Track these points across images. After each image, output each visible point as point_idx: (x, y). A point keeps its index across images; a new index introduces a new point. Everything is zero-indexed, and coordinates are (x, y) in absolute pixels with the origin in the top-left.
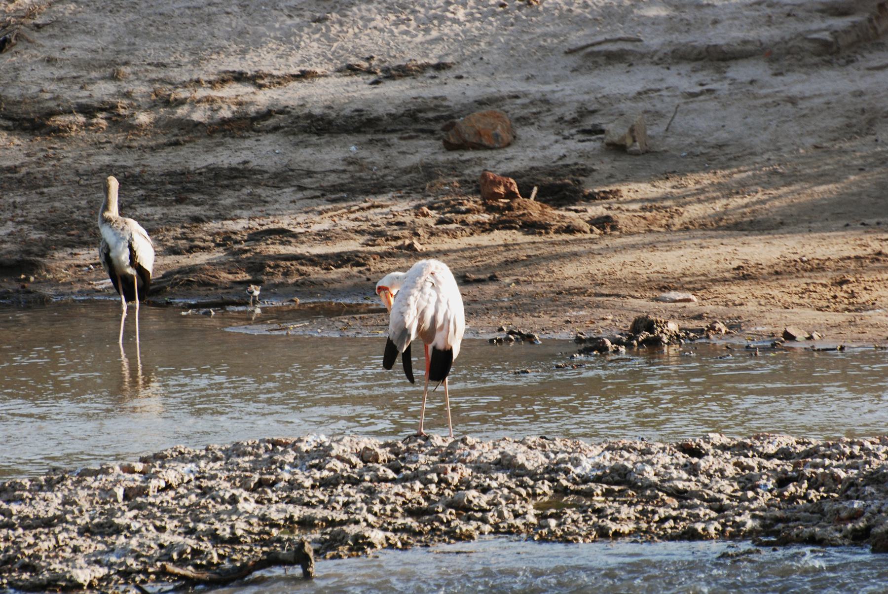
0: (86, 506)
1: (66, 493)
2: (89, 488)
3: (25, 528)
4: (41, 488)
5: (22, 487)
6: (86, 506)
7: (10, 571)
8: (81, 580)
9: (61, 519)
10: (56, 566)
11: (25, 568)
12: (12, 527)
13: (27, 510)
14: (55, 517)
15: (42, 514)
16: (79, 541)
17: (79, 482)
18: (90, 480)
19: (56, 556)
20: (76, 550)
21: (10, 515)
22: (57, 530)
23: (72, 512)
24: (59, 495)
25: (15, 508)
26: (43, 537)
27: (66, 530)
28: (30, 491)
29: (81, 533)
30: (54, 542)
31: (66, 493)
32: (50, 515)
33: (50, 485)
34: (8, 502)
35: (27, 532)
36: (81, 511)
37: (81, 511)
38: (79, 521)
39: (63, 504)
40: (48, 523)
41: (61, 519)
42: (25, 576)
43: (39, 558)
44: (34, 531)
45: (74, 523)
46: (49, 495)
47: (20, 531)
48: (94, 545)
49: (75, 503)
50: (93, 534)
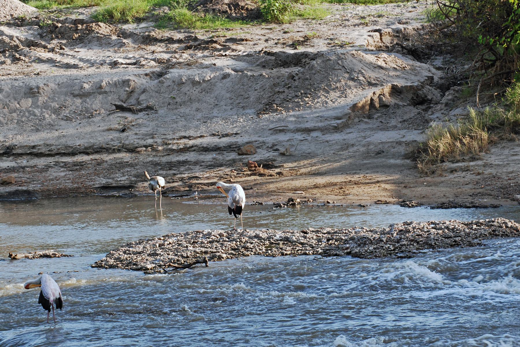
0: (149, 249)
4: (137, 244)
6: (149, 249)
9: (143, 252)
10: (142, 264)
11: (134, 264)
12: (130, 254)
13: (134, 250)
16: (148, 258)
18: (150, 242)
20: (147, 260)
21: (130, 251)
25: (131, 249)
29: (148, 256)
33: (140, 243)
40: (140, 253)
41: (143, 252)
42: (134, 267)
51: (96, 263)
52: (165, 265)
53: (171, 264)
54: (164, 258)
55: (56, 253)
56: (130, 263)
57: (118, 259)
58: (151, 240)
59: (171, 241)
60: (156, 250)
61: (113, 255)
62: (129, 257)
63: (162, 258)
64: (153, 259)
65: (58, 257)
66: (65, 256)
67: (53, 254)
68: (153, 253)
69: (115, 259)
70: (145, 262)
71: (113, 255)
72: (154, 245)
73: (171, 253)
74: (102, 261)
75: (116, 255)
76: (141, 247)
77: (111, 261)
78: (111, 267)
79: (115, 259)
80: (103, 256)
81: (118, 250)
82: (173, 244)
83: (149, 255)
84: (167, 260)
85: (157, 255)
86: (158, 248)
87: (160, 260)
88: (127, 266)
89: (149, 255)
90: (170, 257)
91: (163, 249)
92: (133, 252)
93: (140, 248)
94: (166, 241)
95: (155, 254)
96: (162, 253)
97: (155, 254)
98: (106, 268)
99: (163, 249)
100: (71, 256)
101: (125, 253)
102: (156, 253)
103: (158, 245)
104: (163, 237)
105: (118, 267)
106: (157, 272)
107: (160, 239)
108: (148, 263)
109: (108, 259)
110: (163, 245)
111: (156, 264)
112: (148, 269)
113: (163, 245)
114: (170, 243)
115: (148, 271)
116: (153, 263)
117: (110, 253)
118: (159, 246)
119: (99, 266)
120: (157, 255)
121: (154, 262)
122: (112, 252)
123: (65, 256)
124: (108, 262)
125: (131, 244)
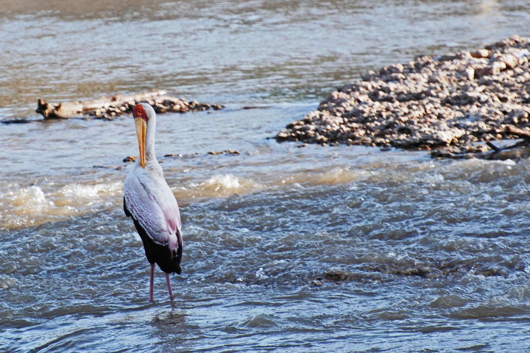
0: (446, 83)
1: (430, 74)
2: (447, 70)
3: (400, 101)
4: (411, 70)
5: (397, 71)
6: (446, 83)
7: (391, 133)
8: (445, 139)
10: (426, 129)
11: (402, 131)
12: (390, 100)
13: (401, 88)
14: (423, 92)
15: (413, 91)
17: (439, 66)
18: (448, 64)
19: (425, 122)
20: (440, 116)
22: (425, 102)
23: (436, 88)
24: (426, 75)
25: (392, 86)
26: (415, 107)
27: (431, 102)
28: (403, 73)
29: (443, 104)
30: (423, 111)
31: (430, 74)
32: (419, 91)
33: (418, 68)
34: (387, 81)
35: (402, 104)
36: (442, 88)
37: (442, 88)
38: (441, 95)
39: (428, 82)
40: (418, 97)
42: (403, 137)
43: (412, 123)
44: (407, 103)
45: (437, 97)
46: (417, 76)
47: (397, 103)
48: (453, 113)
49: (437, 81)
50: (452, 104)
51: (290, 126)
52: (493, 132)
53: (513, 128)
54: (489, 112)
55: (175, 100)
56: (391, 125)
57: (355, 115)
58: (451, 59)
59: (510, 60)
60: (465, 88)
61: (339, 102)
62: (387, 109)
63: (484, 110)
64: (459, 114)
65: (181, 111)
66: (199, 107)
67: (164, 103)
68: (457, 98)
69: (346, 114)
70: (433, 124)
71: (339, 102)
72: (461, 73)
73: (511, 96)
74: (307, 122)
75: (349, 106)
76: (423, 78)
77: (335, 123)
78: (335, 138)
79: (346, 114)
80: (311, 108)
81: (355, 88)
82: (518, 70)
83: (446, 102)
84: (500, 117)
85: (471, 101)
86: (473, 81)
87: (478, 117)
88: (382, 135)
89: (446, 102)
90: (508, 107)
91: (487, 83)
92: (399, 94)
93: (419, 83)
94: (498, 59)
95: (463, 100)
96: (484, 97)
97: (463, 100)
98: (321, 142)
99: (487, 83)
100: (216, 108)
101: (374, 96)
102: (466, 97)
103: (471, 72)
104: (488, 48)
105: (354, 138)
106: (470, 151)
107: (478, 56)
108: (444, 125)
109: (326, 115)
110: (488, 72)
111: (466, 128)
112: (444, 144)
113: (488, 72)
114: (508, 67)
115: (444, 151)
116: (457, 126)
117: (331, 99)
118: (476, 76)
119: (299, 135)
120: (471, 101)
121: (462, 122)
122: (335, 94)
123: (199, 107)
124: (325, 123)
125: (391, 70)
